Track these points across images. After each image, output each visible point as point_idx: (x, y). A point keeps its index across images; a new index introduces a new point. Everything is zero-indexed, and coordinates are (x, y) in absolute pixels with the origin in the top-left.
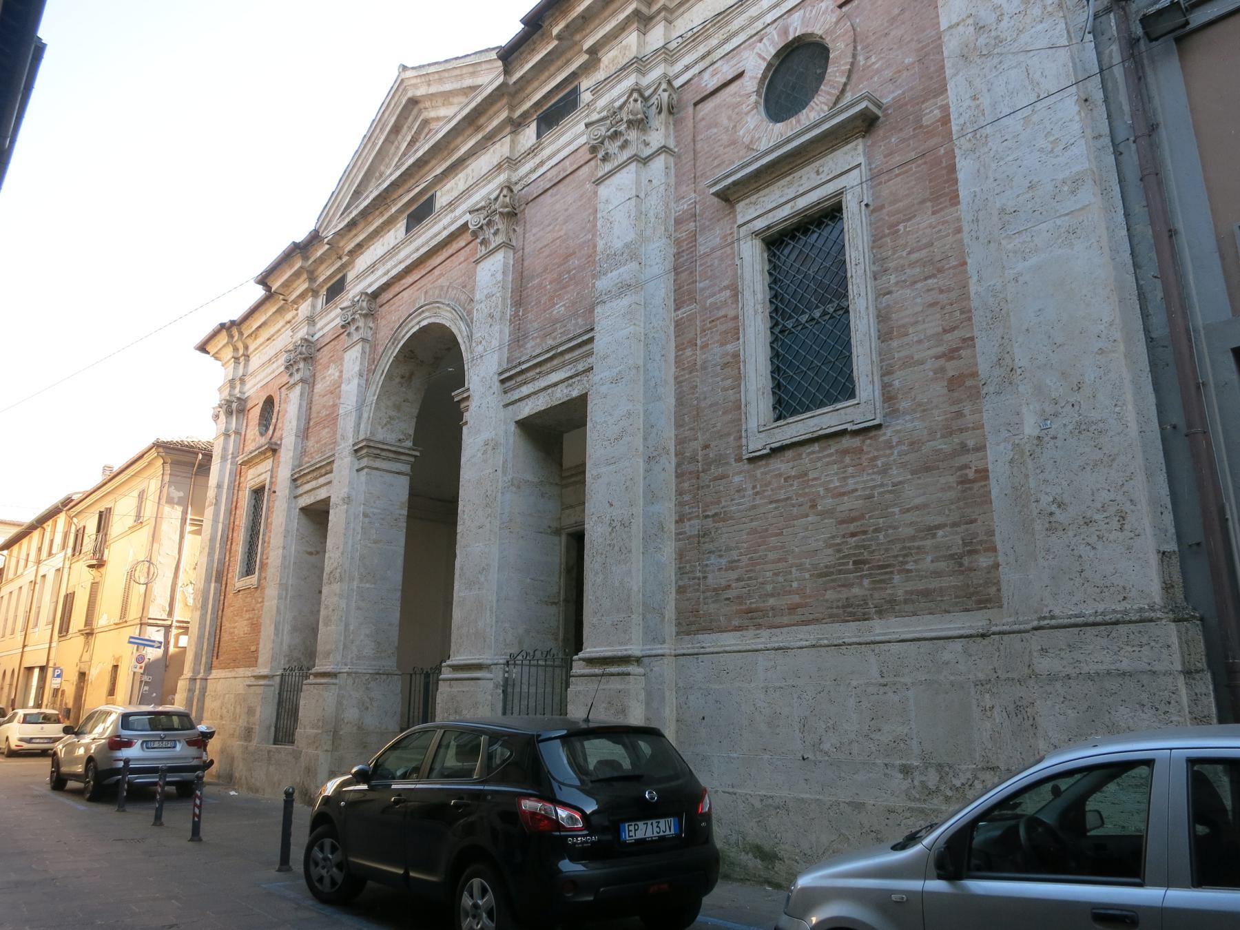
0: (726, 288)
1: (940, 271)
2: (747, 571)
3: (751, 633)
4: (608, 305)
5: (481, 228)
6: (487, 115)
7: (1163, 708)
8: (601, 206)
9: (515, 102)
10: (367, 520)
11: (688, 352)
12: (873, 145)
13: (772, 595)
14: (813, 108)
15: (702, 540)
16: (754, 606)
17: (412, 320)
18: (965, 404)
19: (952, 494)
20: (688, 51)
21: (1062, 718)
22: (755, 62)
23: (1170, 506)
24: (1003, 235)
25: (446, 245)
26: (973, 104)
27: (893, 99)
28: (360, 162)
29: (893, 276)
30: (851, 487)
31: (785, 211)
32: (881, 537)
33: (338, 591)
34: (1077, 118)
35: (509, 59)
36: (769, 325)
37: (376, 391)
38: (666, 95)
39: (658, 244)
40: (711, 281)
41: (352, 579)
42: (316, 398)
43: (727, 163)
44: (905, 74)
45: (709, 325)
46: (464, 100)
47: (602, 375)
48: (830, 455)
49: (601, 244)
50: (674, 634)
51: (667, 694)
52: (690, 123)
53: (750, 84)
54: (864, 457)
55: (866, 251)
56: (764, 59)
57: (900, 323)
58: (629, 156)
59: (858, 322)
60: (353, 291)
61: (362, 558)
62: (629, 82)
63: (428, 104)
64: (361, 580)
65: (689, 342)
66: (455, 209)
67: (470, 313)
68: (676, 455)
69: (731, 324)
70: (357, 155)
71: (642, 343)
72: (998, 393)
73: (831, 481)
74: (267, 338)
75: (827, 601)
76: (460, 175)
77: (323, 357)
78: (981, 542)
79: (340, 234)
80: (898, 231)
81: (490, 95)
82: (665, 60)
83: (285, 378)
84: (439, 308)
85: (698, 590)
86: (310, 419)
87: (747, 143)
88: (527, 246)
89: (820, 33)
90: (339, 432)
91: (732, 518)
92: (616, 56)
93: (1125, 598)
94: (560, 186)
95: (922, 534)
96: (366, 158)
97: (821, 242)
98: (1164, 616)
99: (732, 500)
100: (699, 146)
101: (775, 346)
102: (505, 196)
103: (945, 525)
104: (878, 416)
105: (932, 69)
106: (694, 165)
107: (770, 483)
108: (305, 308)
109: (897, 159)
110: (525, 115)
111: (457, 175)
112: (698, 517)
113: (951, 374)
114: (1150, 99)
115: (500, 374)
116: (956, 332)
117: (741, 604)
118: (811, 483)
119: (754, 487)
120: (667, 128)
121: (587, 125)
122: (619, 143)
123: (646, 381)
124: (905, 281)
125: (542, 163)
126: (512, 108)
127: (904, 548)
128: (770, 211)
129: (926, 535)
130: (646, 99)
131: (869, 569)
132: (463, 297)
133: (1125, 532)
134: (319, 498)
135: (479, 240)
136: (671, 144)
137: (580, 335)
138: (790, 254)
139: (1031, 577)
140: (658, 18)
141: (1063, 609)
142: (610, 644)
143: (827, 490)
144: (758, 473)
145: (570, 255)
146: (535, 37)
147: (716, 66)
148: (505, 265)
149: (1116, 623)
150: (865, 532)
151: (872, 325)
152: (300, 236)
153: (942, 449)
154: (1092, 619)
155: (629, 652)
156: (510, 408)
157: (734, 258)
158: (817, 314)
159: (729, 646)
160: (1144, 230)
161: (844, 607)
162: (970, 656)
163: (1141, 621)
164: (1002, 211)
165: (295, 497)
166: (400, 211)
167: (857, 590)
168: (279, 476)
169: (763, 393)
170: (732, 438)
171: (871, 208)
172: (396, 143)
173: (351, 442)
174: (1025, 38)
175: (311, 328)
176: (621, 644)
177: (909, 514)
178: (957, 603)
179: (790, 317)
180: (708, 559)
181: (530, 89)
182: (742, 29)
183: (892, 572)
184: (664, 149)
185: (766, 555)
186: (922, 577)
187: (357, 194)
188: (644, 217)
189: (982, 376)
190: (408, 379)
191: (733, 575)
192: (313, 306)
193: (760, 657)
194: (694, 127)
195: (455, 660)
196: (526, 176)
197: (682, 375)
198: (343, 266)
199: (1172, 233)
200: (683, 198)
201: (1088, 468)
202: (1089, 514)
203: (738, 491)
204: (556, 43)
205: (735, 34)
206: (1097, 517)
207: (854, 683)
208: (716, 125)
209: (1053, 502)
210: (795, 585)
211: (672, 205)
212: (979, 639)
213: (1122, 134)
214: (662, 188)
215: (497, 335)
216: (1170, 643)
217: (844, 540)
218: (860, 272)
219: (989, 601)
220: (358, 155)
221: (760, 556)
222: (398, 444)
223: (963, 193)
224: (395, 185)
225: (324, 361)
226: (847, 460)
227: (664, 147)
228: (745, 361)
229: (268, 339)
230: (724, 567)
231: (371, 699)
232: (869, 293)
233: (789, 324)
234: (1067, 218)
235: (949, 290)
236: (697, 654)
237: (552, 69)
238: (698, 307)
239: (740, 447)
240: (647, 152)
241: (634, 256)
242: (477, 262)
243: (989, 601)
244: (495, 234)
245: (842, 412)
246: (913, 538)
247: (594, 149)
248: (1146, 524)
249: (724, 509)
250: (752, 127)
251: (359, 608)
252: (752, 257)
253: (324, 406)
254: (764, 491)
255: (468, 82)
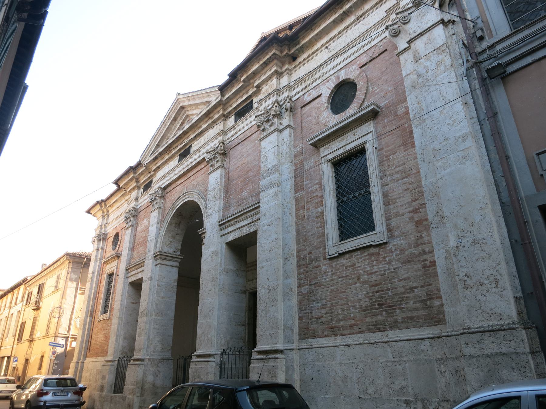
0: (317, 184)
1: (409, 175)
2: (330, 309)
3: (333, 338)
4: (266, 192)
5: (211, 160)
7: (523, 370)
8: (262, 150)
9: (226, 107)
10: (159, 288)
11: (301, 212)
12: (377, 123)
13: (342, 320)
14: (351, 109)
15: (310, 295)
16: (334, 325)
17: (181, 199)
18: (423, 232)
19: (420, 273)
20: (298, 86)
21: (477, 376)
22: (326, 90)
23: (517, 276)
24: (435, 160)
25: (195, 167)
26: (418, 106)
27: (385, 104)
28: (159, 133)
29: (389, 178)
30: (375, 270)
31: (341, 151)
32: (390, 293)
33: (145, 321)
34: (463, 111)
35: (223, 90)
36: (336, 199)
37: (164, 230)
38: (289, 104)
39: (287, 166)
40: (310, 181)
41: (151, 315)
42: (138, 233)
43: (315, 131)
44: (389, 94)
45: (310, 200)
46: (204, 107)
47: (264, 222)
48: (366, 256)
49: (262, 166)
50: (298, 339)
51: (295, 367)
52: (300, 116)
53: (324, 99)
54: (380, 257)
55: (377, 167)
56: (330, 89)
57: (393, 198)
58: (274, 129)
59: (375, 197)
60: (155, 187)
61: (157, 305)
62: (273, 99)
63: (188, 109)
64: (156, 315)
65: (302, 207)
66: (200, 152)
67: (206, 196)
68: (297, 257)
69: (319, 199)
70: (158, 130)
71: (281, 208)
72: (438, 228)
73: (366, 268)
74: (117, 207)
75: (367, 322)
76: (202, 138)
77: (141, 215)
78: (434, 294)
79: (150, 163)
80: (390, 158)
81: (215, 105)
82: (288, 90)
83: (124, 225)
84: (192, 194)
85: (308, 318)
86: (135, 243)
87: (324, 123)
88: (230, 167)
89: (353, 78)
90: (148, 248)
91: (322, 285)
92: (268, 89)
93: (501, 319)
94: (245, 141)
95: (408, 291)
96: (162, 131)
97: (357, 163)
98: (519, 326)
99: (323, 277)
100: (303, 124)
101: (339, 208)
102: (221, 146)
103: (418, 287)
104: (386, 238)
105: (400, 92)
106: (302, 132)
107: (339, 269)
108: (134, 194)
109: (388, 129)
110: (230, 113)
111: (200, 138)
112: (307, 285)
113: (416, 219)
114: (493, 102)
115: (219, 222)
116: (417, 201)
117: (328, 325)
118: (357, 269)
119: (332, 271)
120: (290, 117)
121: (256, 117)
122: (269, 124)
123: (283, 224)
124: (394, 180)
125: (237, 132)
126: (224, 110)
127: (400, 298)
128: (335, 151)
129: (410, 291)
130: (281, 106)
131: (385, 307)
132: (203, 189)
133: (498, 289)
134: (138, 278)
135: (210, 165)
136: (292, 124)
137: (254, 205)
138: (344, 169)
139: (458, 310)
140: (285, 73)
141: (474, 324)
142: (269, 344)
143: (365, 272)
144: (334, 265)
145: (249, 171)
146: (234, 81)
147: (309, 92)
148: (221, 175)
149: (498, 330)
150: (382, 291)
151: (381, 199)
152: (133, 164)
153: (414, 253)
154: (487, 329)
155: (278, 348)
156: (223, 237)
157: (320, 171)
158: (357, 194)
159: (323, 344)
160: (495, 156)
161: (374, 325)
162: (433, 347)
163: (509, 329)
164: (434, 149)
165: (127, 278)
166: (176, 153)
167: (380, 317)
168: (120, 268)
169: (335, 229)
170: (321, 249)
171: (378, 149)
172: (175, 125)
173: (152, 253)
174: (438, 79)
175: (137, 203)
176: (274, 344)
177: (402, 282)
178: (425, 323)
179: (345, 196)
180: (313, 304)
181: (231, 102)
182: (320, 77)
183: (395, 309)
184: (289, 126)
185: (338, 302)
186: (409, 311)
187: (158, 146)
188: (281, 154)
189: (430, 220)
190: (178, 225)
191: (324, 311)
192: (138, 193)
193: (337, 349)
194: (301, 117)
195: (198, 352)
196: (230, 138)
197: (299, 222)
198: (151, 176)
199: (507, 157)
200: (297, 146)
201: (480, 260)
202: (482, 281)
203: (325, 273)
204: (242, 83)
205: (317, 79)
206: (485, 282)
207: (381, 361)
208: (310, 116)
209: (466, 275)
210: (352, 315)
211: (293, 149)
212: (437, 339)
213: (482, 117)
214: (288, 142)
215: (218, 205)
216: (523, 339)
217: (373, 294)
218: (375, 176)
219: (440, 321)
220: (159, 130)
221: (336, 302)
222: (173, 253)
223: (416, 143)
224: (174, 142)
225: (142, 217)
226: (373, 258)
227: (289, 125)
228: (326, 215)
229: (117, 208)
230: (320, 307)
231: (159, 372)
232: (379, 185)
233: (345, 199)
234: (461, 152)
235: (413, 183)
236: (309, 348)
237: (241, 94)
238: (305, 192)
239: (325, 253)
240: (282, 127)
241: (277, 171)
242: (209, 174)
243: (440, 321)
244: (217, 162)
245: (370, 237)
246: (404, 293)
247: (259, 127)
248: (508, 285)
249: (319, 281)
250: (326, 117)
251: (154, 328)
252: (327, 170)
253: (141, 237)
254: (337, 273)
255: (206, 100)
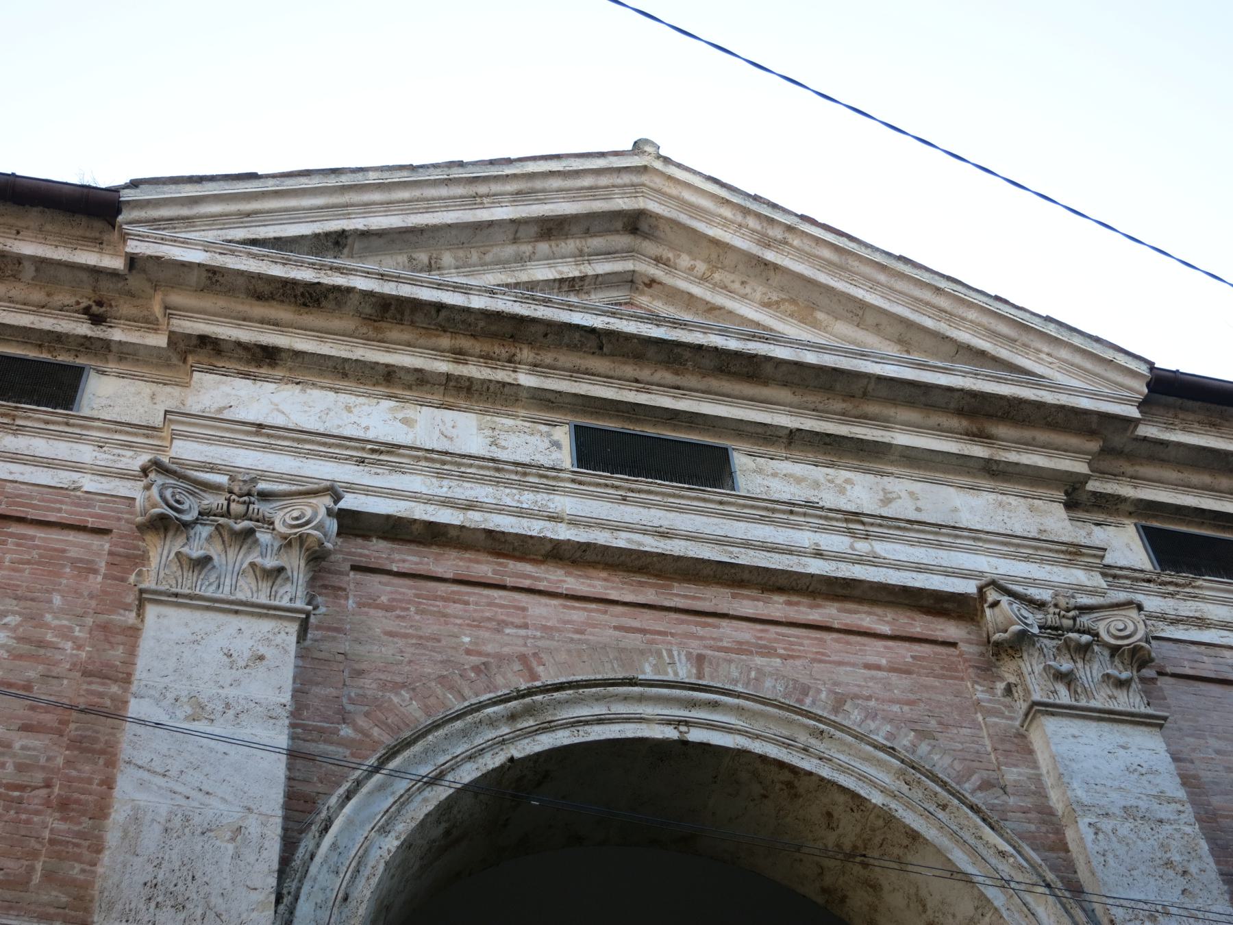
6: (1027, 434)
96: (429, 205)
111: (831, 465)
172: (526, 249)
